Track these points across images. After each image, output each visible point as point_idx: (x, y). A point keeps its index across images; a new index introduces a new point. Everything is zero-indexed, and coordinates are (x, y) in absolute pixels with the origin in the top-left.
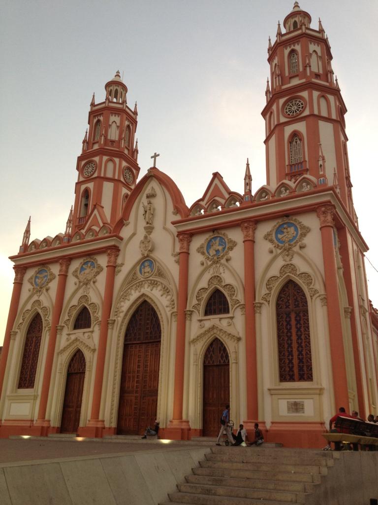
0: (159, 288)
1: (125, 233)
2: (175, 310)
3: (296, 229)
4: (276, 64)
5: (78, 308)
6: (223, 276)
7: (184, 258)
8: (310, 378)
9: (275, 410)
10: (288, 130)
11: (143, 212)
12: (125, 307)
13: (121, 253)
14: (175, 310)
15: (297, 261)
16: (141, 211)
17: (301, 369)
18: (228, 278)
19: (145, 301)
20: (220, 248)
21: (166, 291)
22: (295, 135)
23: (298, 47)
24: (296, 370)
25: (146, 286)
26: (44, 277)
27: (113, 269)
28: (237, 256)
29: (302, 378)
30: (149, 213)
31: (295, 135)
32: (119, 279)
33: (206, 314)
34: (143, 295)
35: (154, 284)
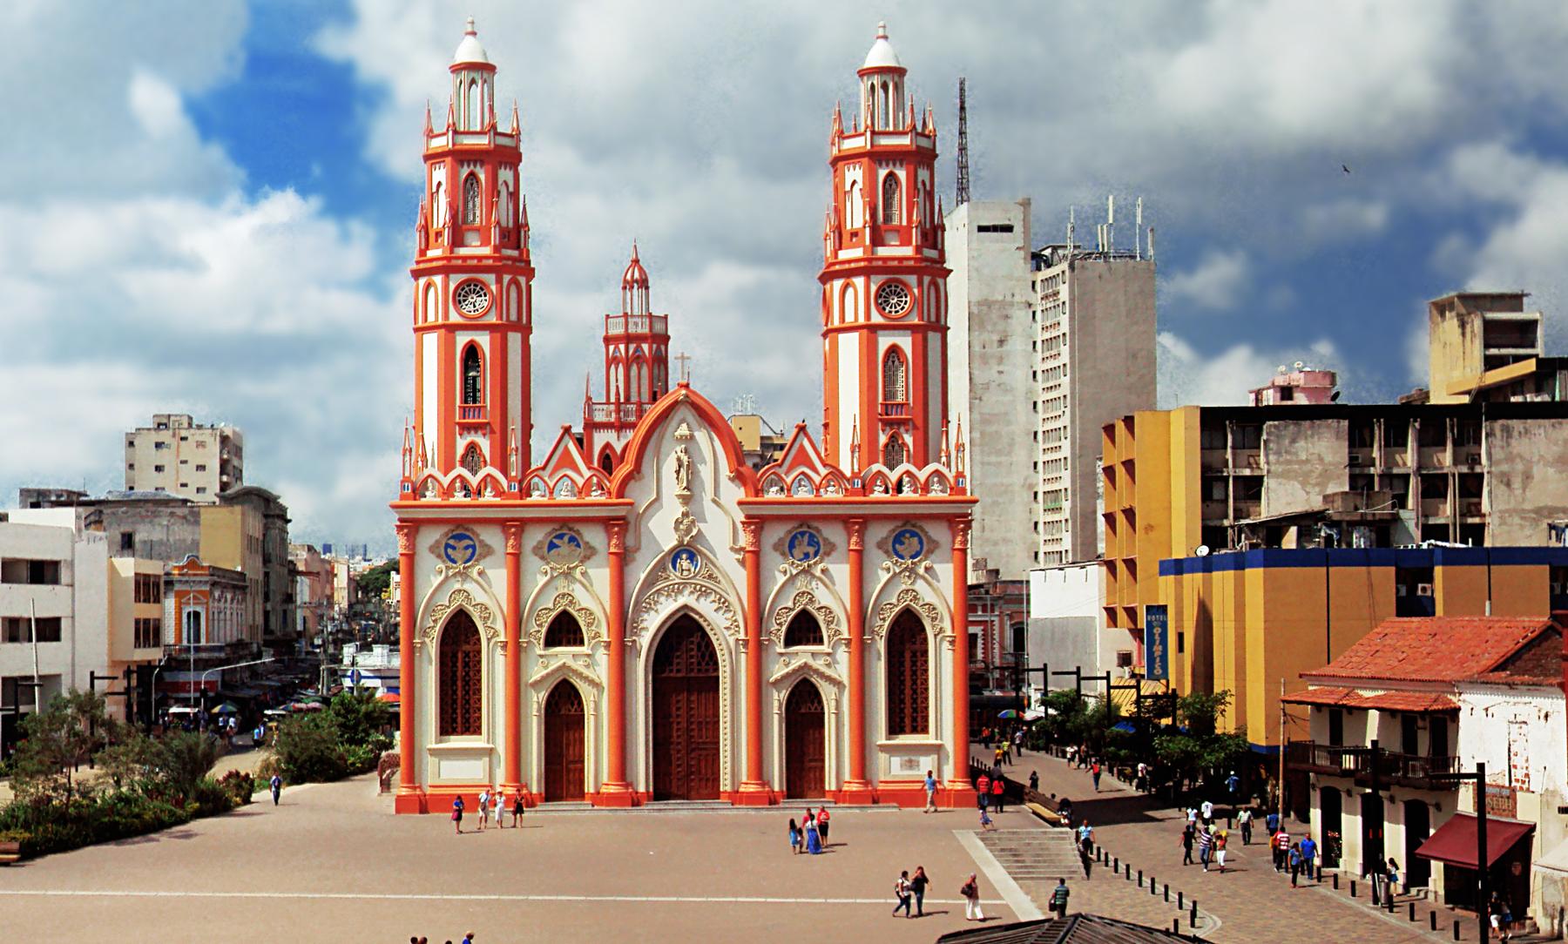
0: (712, 597)
1: (641, 495)
2: (742, 636)
3: (921, 542)
4: (854, 182)
5: (554, 614)
6: (816, 593)
7: (755, 562)
8: (925, 730)
9: (890, 769)
10: (884, 342)
11: (675, 466)
12: (652, 623)
13: (631, 528)
14: (742, 636)
15: (920, 586)
16: (670, 466)
17: (914, 720)
18: (823, 597)
19: (686, 616)
20: (811, 550)
21: (724, 605)
22: (894, 350)
23: (902, 174)
24: (907, 721)
25: (686, 592)
26: (467, 548)
27: (622, 561)
28: (842, 572)
29: (914, 730)
30: (688, 470)
31: (894, 350)
32: (639, 574)
33: (788, 643)
34: (685, 607)
35: (704, 592)
